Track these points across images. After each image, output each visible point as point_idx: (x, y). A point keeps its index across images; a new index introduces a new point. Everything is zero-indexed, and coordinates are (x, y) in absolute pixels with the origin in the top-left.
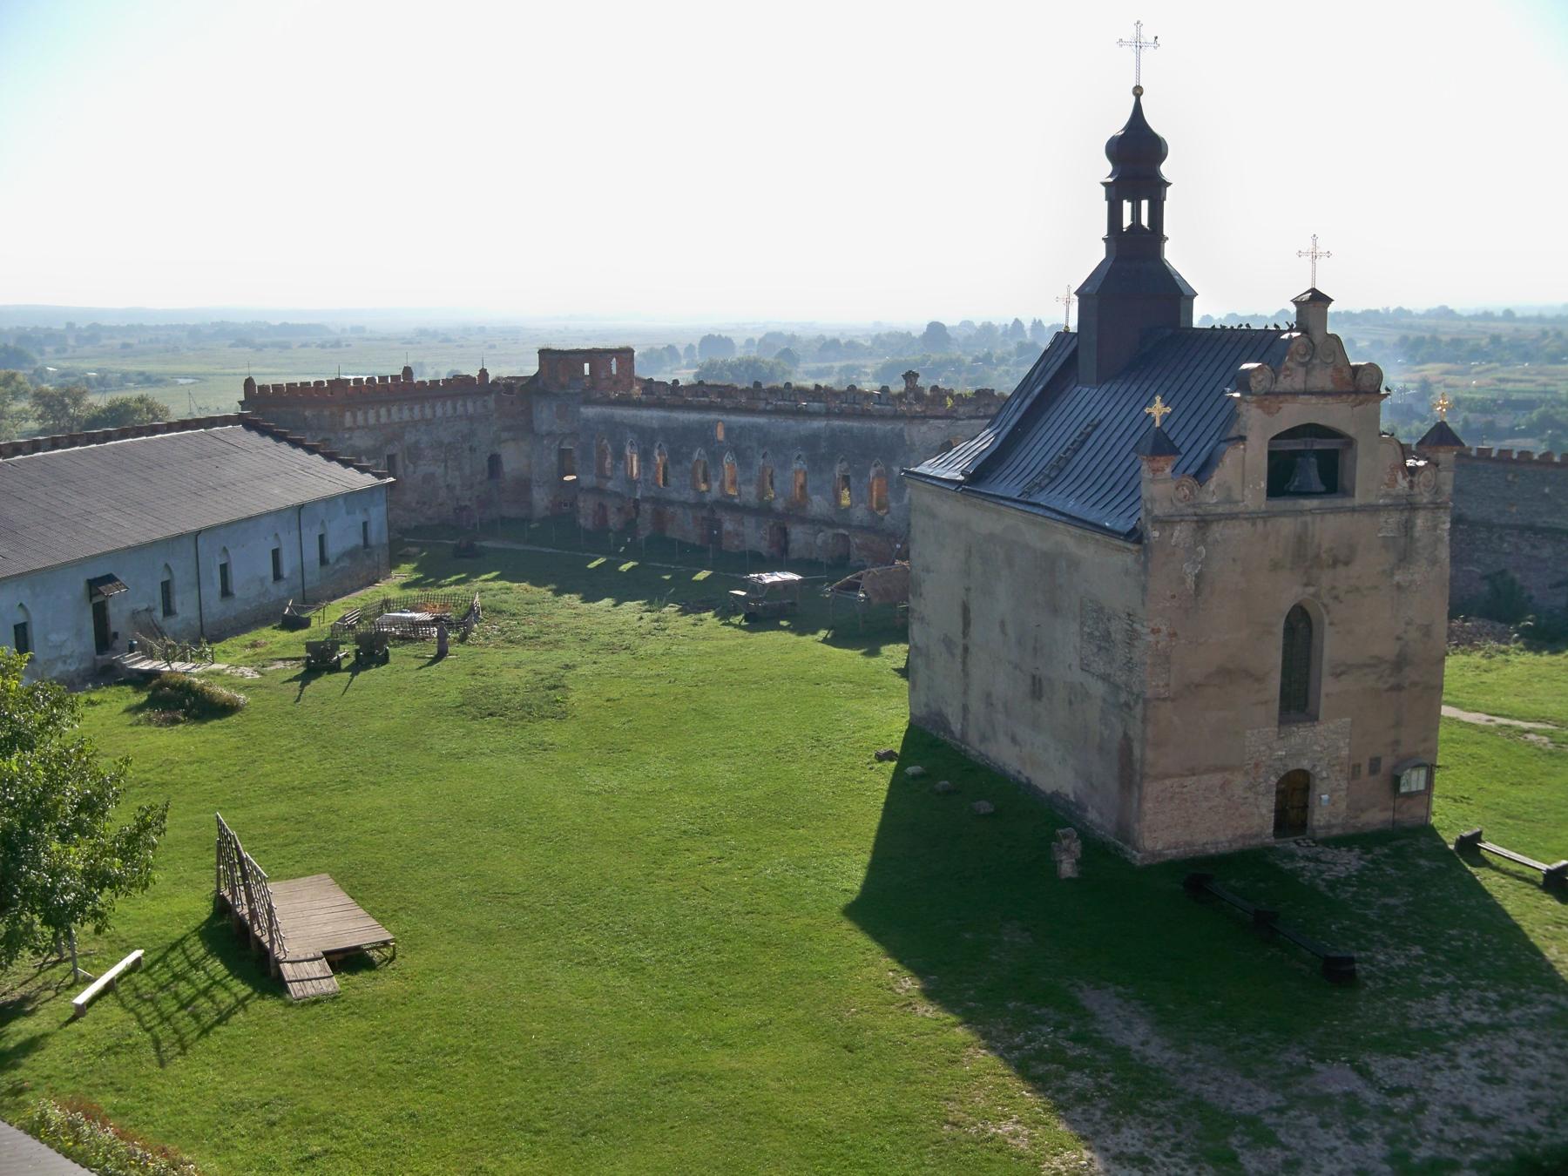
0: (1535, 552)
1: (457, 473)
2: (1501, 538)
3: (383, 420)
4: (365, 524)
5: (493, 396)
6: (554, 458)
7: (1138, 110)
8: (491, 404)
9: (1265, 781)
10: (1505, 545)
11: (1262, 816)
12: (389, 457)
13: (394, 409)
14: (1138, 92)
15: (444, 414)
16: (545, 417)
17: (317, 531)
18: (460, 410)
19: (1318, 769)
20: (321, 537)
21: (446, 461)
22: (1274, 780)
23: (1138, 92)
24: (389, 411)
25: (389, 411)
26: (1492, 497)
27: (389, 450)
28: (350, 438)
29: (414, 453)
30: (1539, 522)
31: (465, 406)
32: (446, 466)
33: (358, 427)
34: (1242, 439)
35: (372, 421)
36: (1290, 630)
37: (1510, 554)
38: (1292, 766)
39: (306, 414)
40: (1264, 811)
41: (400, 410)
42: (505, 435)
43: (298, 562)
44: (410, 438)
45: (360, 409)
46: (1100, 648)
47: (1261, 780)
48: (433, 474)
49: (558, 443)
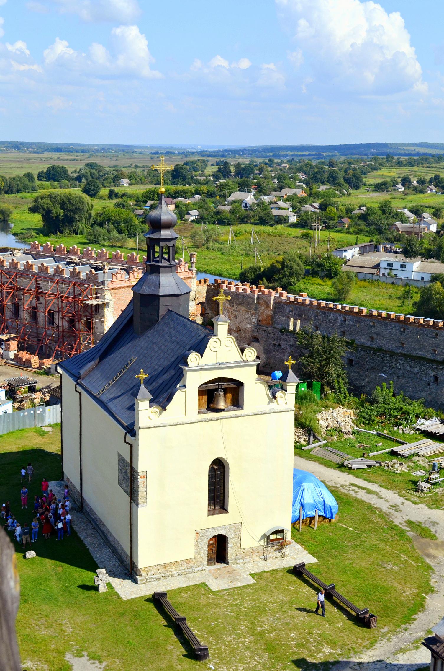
2: (396, 360)
9: (203, 540)
10: (398, 365)
22: (206, 541)
30: (415, 353)
34: (185, 386)
36: (212, 470)
37: (400, 369)
40: (202, 555)
46: (124, 478)
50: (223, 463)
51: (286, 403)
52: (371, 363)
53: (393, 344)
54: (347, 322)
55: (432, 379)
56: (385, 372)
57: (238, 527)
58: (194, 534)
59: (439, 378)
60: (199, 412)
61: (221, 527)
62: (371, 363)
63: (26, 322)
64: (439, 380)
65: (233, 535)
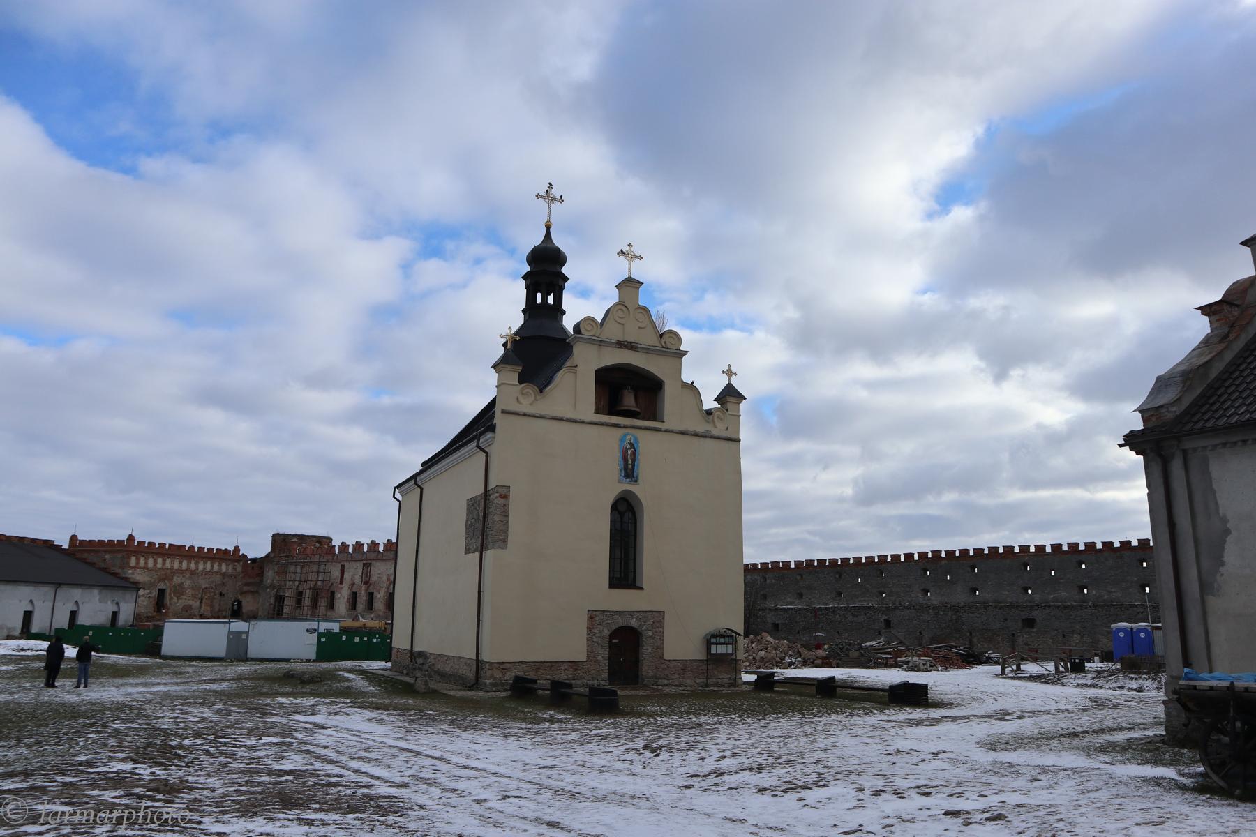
0: (856, 619)
1: (209, 608)
3: (159, 566)
4: (115, 614)
5: (241, 563)
6: (272, 601)
7: (548, 235)
8: (239, 568)
9: (600, 632)
10: (837, 616)
11: (597, 661)
12: (159, 589)
13: (168, 561)
14: (548, 227)
15: (205, 569)
16: (270, 575)
17: (71, 607)
18: (216, 567)
19: (644, 628)
20: (73, 615)
21: (202, 600)
22: (606, 632)
23: (548, 227)
24: (164, 561)
25: (164, 561)
26: (828, 589)
27: (161, 586)
28: (133, 573)
29: (179, 591)
31: (220, 565)
32: (201, 603)
33: (140, 568)
35: (151, 563)
37: (840, 622)
38: (622, 622)
39: (106, 557)
40: (600, 658)
41: (172, 562)
42: (246, 588)
43: (48, 624)
44: (177, 580)
45: (143, 556)
47: (596, 631)
48: (191, 606)
49: (275, 590)
50: (633, 508)
51: (727, 429)
52: (803, 621)
53: (828, 595)
54: (768, 582)
55: (883, 625)
56: (821, 630)
57: (658, 618)
58: (586, 617)
59: (892, 622)
60: (597, 411)
61: (631, 613)
62: (803, 621)
63: (381, 613)
64: (892, 625)
65: (650, 633)
